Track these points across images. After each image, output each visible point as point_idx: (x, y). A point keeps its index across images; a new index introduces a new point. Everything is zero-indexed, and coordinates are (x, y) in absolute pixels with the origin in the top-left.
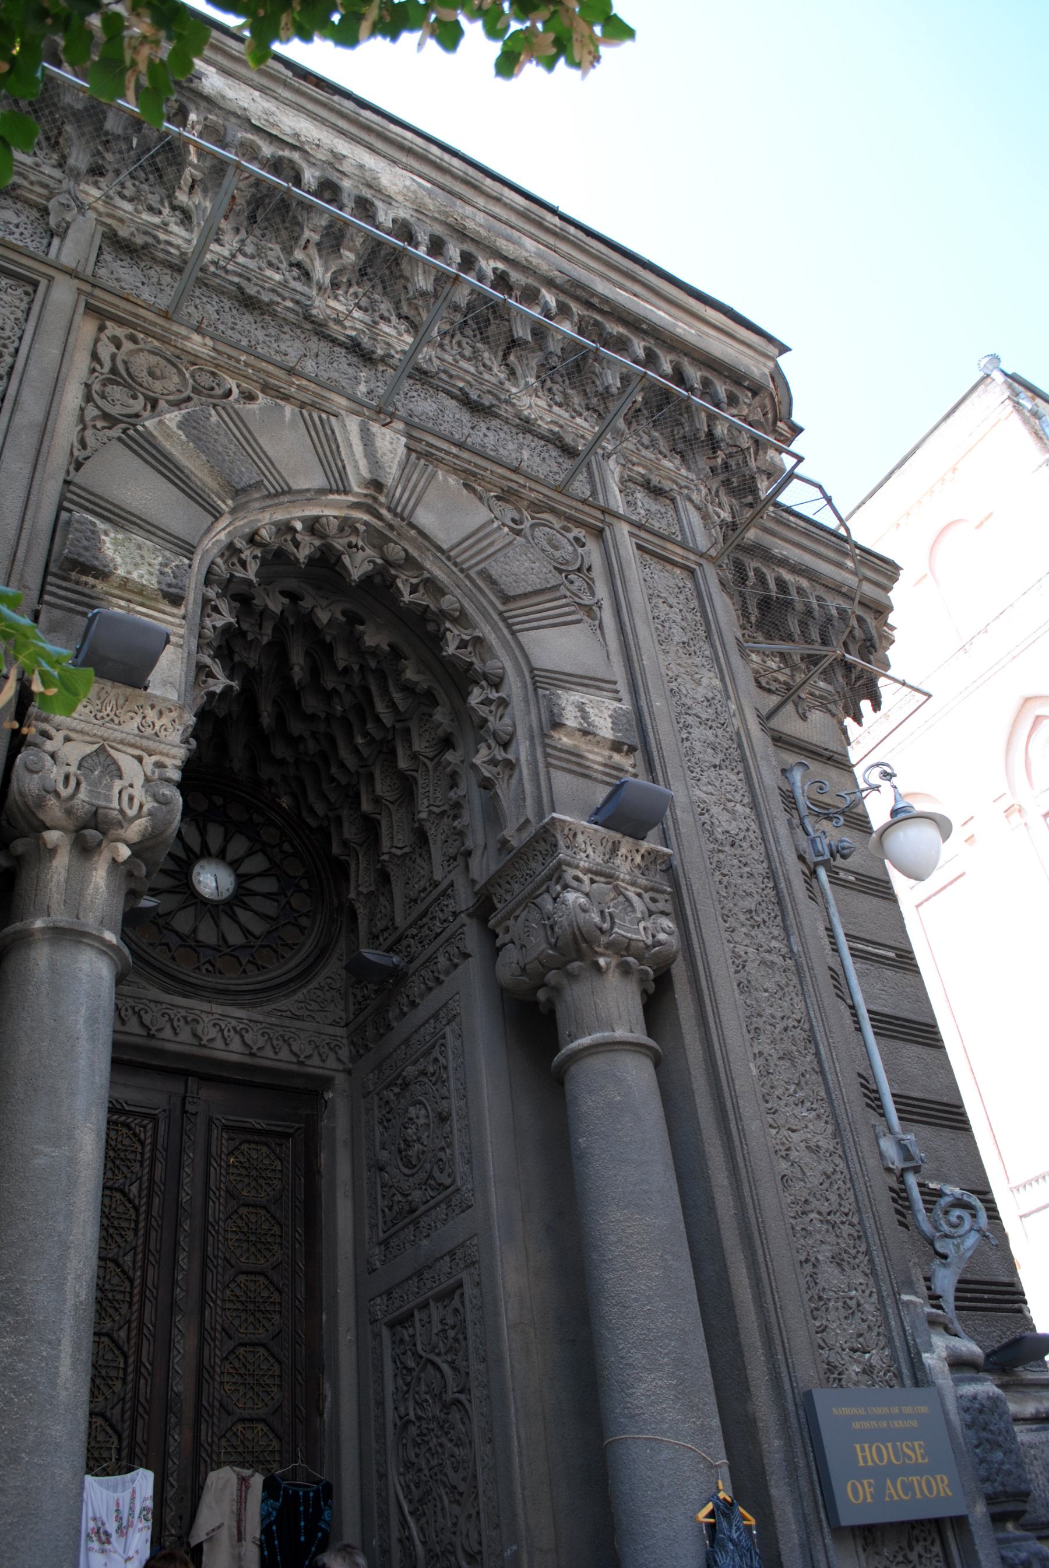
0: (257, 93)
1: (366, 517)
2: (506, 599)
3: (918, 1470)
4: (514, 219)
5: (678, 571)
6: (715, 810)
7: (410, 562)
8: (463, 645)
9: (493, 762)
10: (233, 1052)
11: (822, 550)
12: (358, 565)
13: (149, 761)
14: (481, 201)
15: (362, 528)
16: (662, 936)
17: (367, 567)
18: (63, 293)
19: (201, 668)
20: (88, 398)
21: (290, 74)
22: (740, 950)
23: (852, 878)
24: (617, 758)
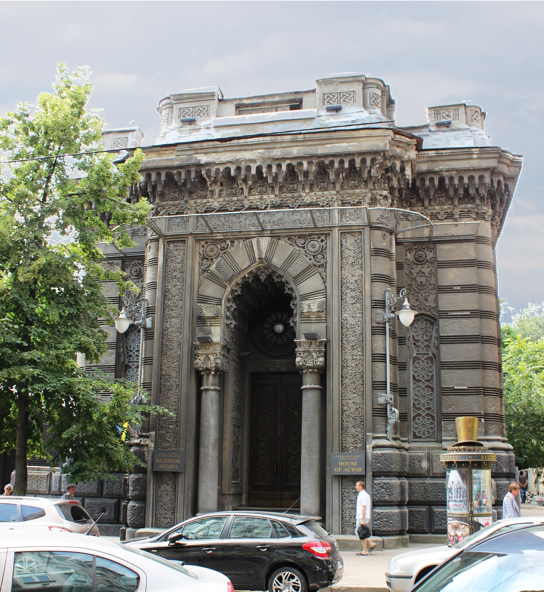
0: (214, 154)
1: (262, 265)
2: (294, 278)
3: (354, 467)
4: (290, 144)
5: (357, 234)
6: (349, 319)
7: (274, 272)
8: (289, 289)
9: (293, 322)
10: (285, 369)
11: (461, 157)
12: (263, 278)
13: (215, 355)
14: (278, 146)
15: (262, 268)
16: (318, 363)
17: (265, 276)
18: (190, 240)
19: (227, 325)
20: (200, 267)
21: (219, 143)
22: (346, 357)
23: (459, 288)
24: (320, 314)
